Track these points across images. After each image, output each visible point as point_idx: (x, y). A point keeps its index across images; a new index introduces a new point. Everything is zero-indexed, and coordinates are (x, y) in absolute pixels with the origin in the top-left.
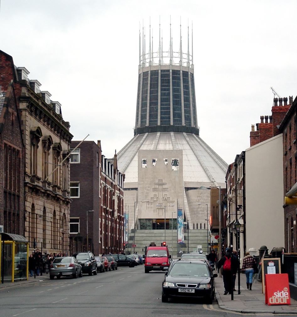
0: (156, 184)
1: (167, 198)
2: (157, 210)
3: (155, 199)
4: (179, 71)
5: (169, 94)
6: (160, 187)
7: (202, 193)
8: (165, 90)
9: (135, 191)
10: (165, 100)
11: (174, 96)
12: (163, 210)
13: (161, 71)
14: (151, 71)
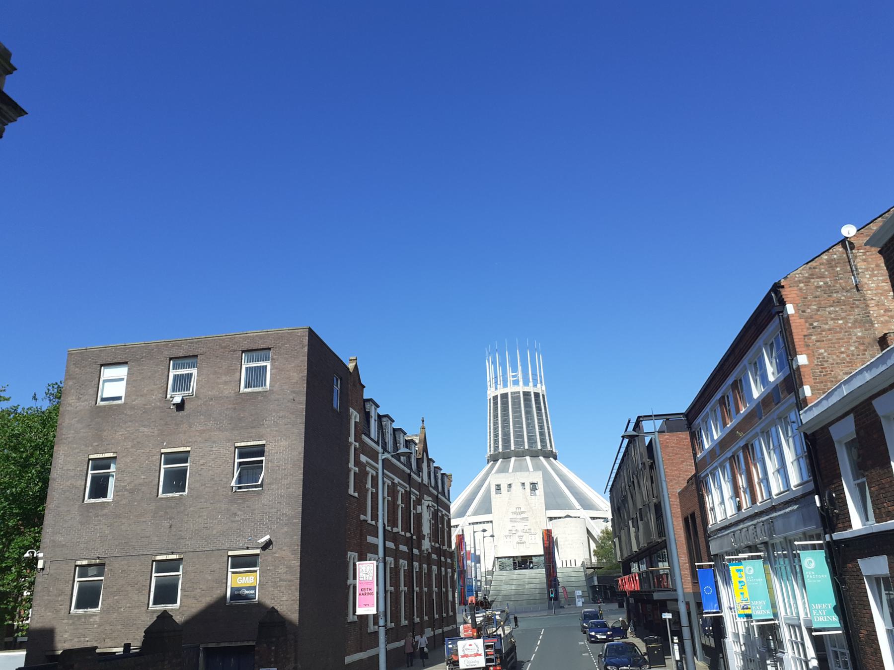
0: (514, 513)
3: (514, 532)
4: (529, 392)
5: (521, 416)
6: (519, 517)
9: (491, 524)
10: (518, 423)
11: (527, 419)
12: (525, 544)
13: (511, 393)
14: (501, 395)
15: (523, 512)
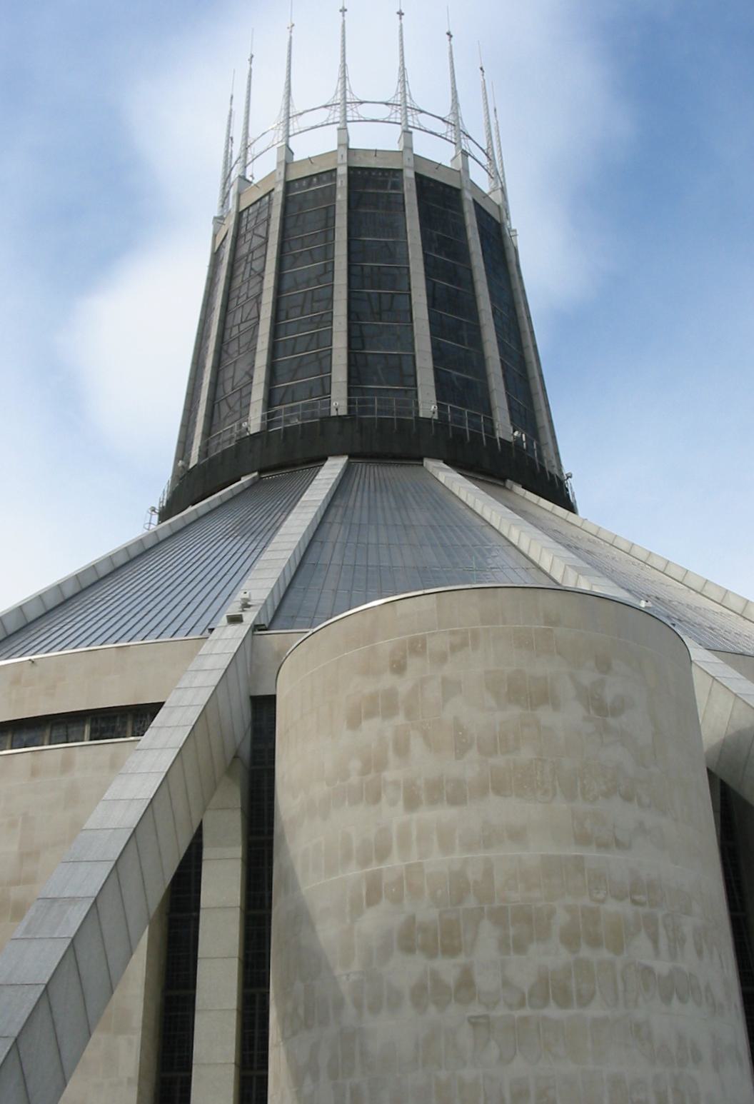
7: (417, 647)
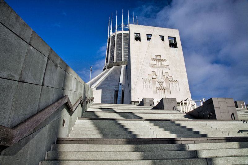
0: (153, 59)
1: (168, 77)
2: (158, 90)
8: (126, 43)
15: (163, 60)
